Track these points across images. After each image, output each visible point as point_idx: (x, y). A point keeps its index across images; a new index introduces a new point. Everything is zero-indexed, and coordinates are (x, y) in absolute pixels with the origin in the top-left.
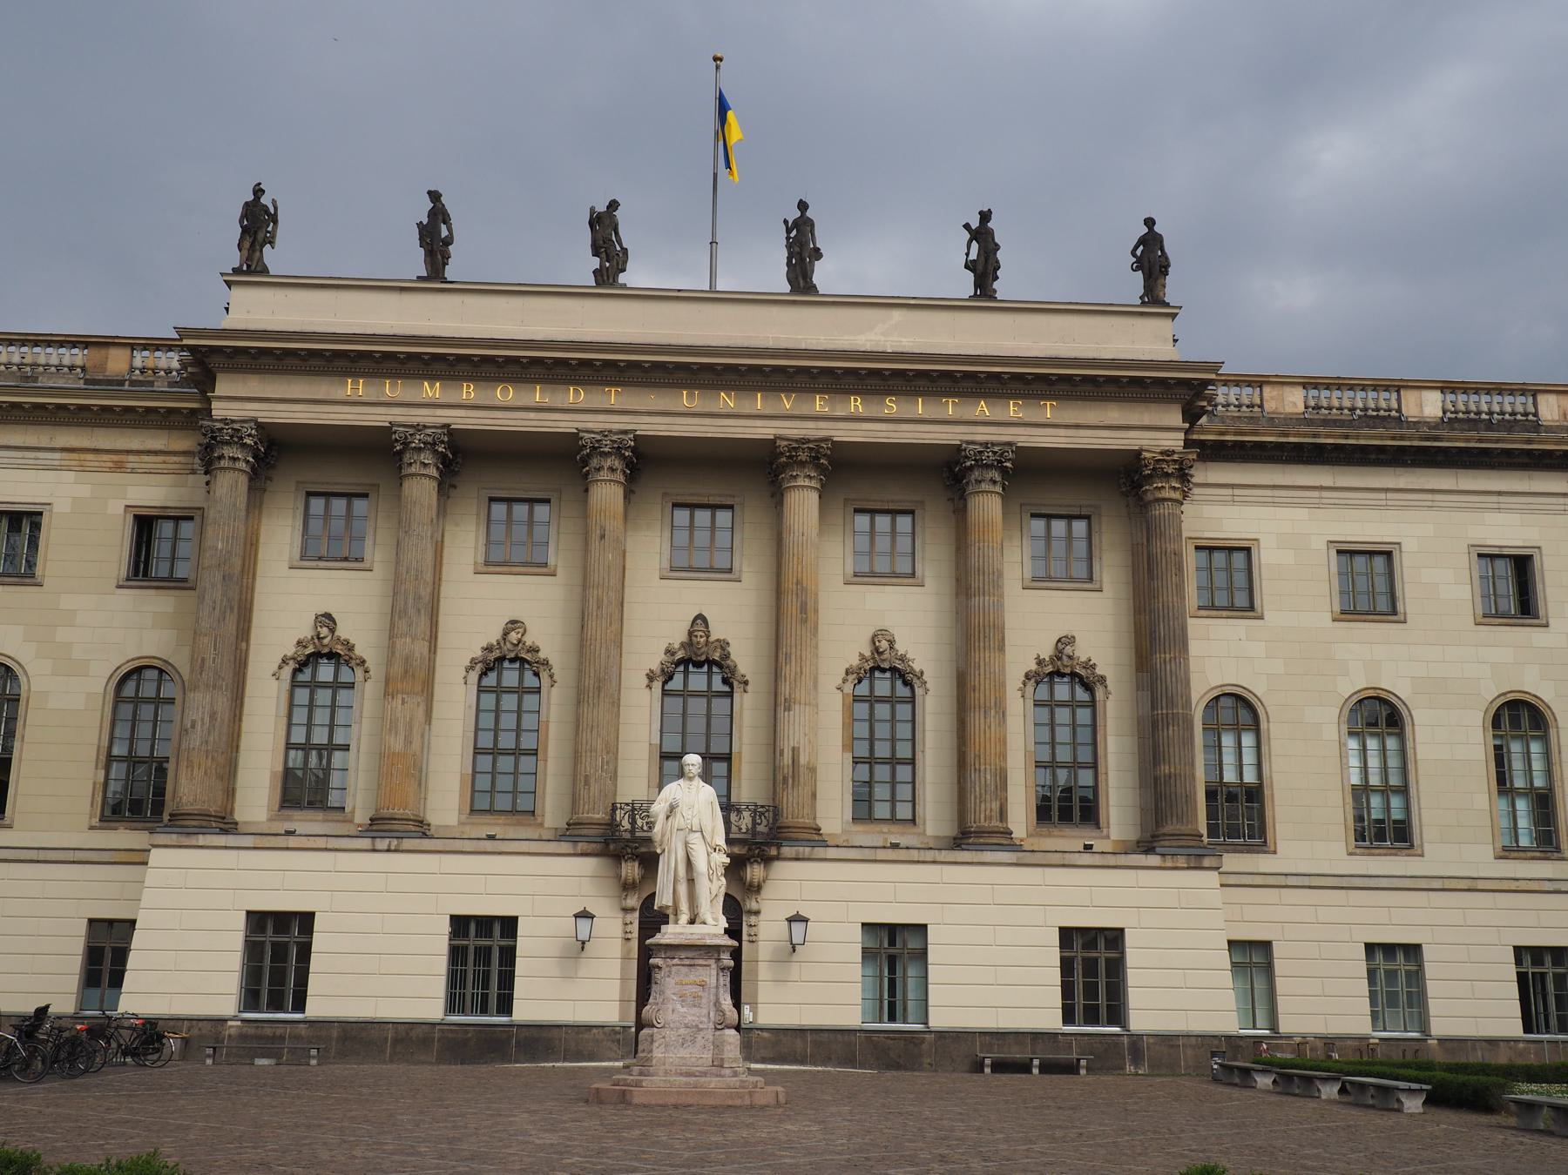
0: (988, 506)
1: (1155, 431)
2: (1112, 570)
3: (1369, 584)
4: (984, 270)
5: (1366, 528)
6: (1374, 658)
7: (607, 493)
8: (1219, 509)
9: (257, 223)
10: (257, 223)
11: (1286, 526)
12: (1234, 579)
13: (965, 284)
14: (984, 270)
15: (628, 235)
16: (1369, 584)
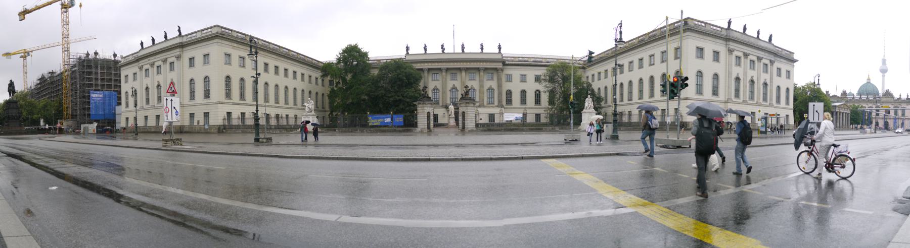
0: (482, 73)
1: (500, 66)
2: (495, 78)
3: (523, 78)
4: (482, 49)
5: (524, 73)
6: (523, 86)
7: (444, 73)
8: (509, 71)
9: (408, 48)
10: (408, 48)
11: (516, 73)
12: (509, 78)
13: (480, 51)
14: (482, 49)
15: (445, 47)
16: (523, 78)
